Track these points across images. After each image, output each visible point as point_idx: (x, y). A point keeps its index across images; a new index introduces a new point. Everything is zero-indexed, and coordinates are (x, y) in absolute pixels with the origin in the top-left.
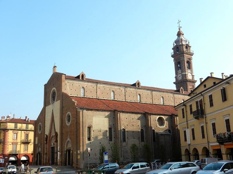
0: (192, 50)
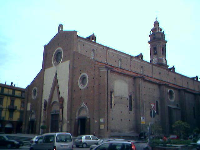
0: (166, 38)
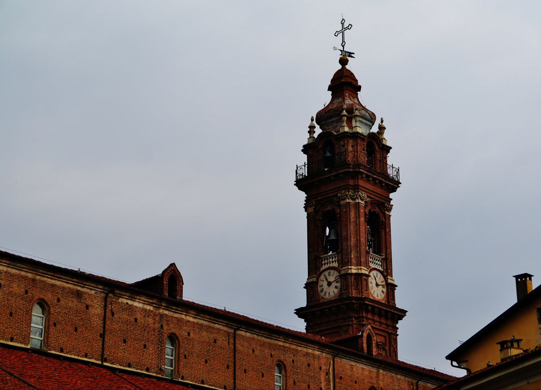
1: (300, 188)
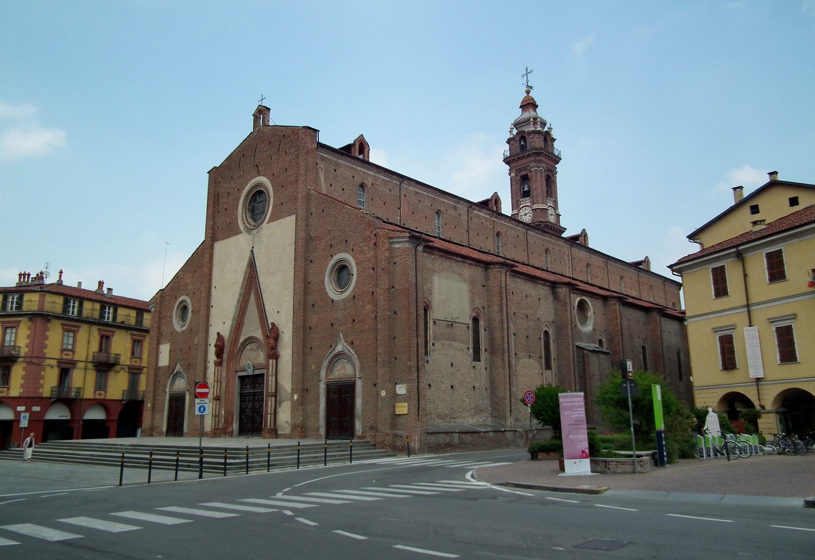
0: (559, 147)
1: (507, 163)
